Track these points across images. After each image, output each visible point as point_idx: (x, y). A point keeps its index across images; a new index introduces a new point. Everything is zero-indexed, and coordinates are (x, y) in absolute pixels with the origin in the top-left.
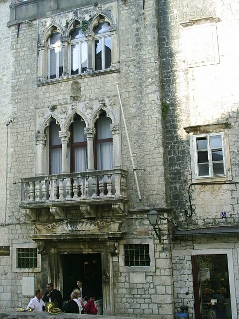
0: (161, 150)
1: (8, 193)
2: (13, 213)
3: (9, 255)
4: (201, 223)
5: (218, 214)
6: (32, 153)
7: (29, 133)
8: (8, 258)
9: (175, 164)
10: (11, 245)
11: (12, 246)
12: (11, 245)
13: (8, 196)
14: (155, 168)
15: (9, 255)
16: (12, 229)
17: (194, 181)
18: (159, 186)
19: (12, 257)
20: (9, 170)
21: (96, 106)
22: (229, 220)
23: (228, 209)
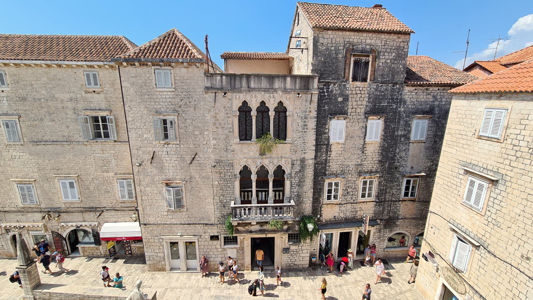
0: (312, 190)
1: (216, 207)
2: (220, 219)
3: (218, 240)
4: (324, 221)
5: (332, 217)
6: (232, 185)
7: (229, 174)
8: (219, 242)
9: (316, 195)
10: (219, 235)
11: (220, 235)
12: (219, 235)
13: (216, 210)
14: (307, 199)
15: (218, 240)
16: (220, 227)
17: (324, 203)
18: (310, 208)
19: (221, 241)
20: (215, 194)
21: (276, 163)
22: (337, 219)
23: (337, 215)
